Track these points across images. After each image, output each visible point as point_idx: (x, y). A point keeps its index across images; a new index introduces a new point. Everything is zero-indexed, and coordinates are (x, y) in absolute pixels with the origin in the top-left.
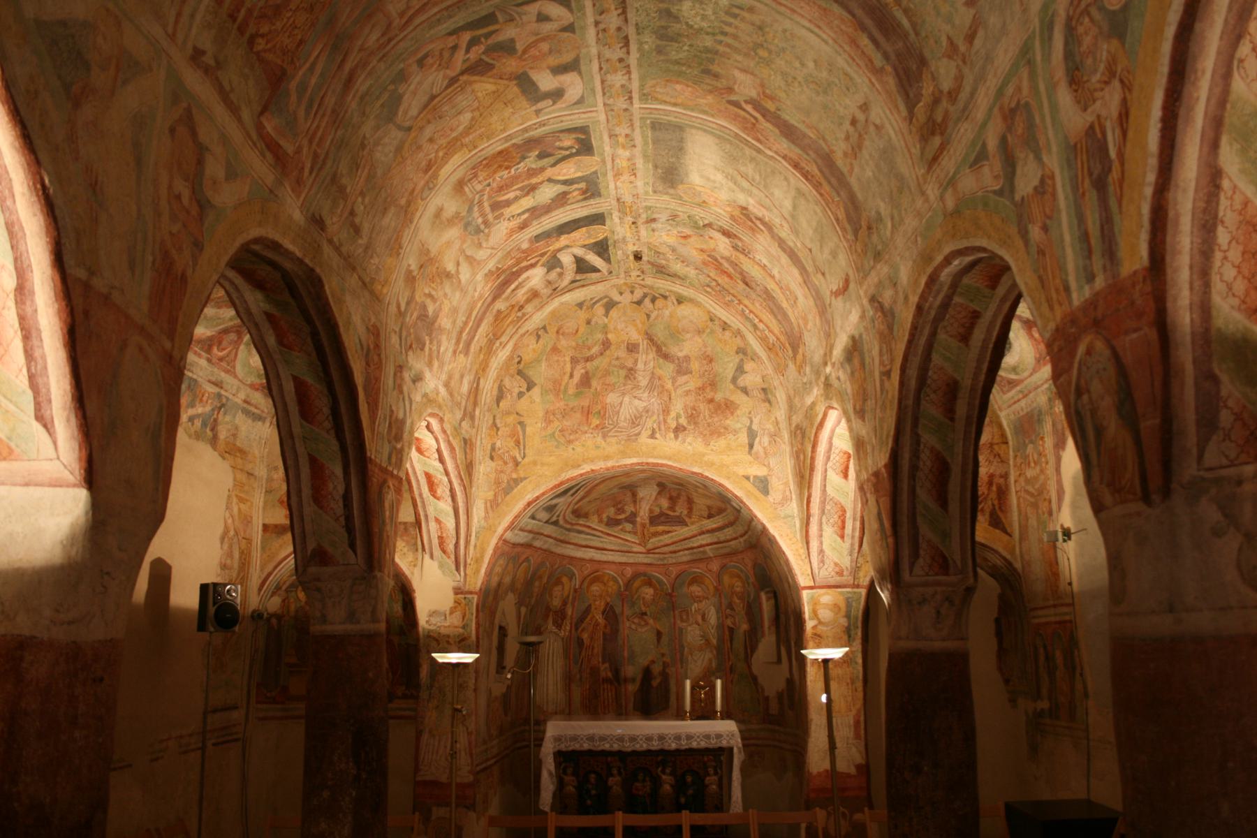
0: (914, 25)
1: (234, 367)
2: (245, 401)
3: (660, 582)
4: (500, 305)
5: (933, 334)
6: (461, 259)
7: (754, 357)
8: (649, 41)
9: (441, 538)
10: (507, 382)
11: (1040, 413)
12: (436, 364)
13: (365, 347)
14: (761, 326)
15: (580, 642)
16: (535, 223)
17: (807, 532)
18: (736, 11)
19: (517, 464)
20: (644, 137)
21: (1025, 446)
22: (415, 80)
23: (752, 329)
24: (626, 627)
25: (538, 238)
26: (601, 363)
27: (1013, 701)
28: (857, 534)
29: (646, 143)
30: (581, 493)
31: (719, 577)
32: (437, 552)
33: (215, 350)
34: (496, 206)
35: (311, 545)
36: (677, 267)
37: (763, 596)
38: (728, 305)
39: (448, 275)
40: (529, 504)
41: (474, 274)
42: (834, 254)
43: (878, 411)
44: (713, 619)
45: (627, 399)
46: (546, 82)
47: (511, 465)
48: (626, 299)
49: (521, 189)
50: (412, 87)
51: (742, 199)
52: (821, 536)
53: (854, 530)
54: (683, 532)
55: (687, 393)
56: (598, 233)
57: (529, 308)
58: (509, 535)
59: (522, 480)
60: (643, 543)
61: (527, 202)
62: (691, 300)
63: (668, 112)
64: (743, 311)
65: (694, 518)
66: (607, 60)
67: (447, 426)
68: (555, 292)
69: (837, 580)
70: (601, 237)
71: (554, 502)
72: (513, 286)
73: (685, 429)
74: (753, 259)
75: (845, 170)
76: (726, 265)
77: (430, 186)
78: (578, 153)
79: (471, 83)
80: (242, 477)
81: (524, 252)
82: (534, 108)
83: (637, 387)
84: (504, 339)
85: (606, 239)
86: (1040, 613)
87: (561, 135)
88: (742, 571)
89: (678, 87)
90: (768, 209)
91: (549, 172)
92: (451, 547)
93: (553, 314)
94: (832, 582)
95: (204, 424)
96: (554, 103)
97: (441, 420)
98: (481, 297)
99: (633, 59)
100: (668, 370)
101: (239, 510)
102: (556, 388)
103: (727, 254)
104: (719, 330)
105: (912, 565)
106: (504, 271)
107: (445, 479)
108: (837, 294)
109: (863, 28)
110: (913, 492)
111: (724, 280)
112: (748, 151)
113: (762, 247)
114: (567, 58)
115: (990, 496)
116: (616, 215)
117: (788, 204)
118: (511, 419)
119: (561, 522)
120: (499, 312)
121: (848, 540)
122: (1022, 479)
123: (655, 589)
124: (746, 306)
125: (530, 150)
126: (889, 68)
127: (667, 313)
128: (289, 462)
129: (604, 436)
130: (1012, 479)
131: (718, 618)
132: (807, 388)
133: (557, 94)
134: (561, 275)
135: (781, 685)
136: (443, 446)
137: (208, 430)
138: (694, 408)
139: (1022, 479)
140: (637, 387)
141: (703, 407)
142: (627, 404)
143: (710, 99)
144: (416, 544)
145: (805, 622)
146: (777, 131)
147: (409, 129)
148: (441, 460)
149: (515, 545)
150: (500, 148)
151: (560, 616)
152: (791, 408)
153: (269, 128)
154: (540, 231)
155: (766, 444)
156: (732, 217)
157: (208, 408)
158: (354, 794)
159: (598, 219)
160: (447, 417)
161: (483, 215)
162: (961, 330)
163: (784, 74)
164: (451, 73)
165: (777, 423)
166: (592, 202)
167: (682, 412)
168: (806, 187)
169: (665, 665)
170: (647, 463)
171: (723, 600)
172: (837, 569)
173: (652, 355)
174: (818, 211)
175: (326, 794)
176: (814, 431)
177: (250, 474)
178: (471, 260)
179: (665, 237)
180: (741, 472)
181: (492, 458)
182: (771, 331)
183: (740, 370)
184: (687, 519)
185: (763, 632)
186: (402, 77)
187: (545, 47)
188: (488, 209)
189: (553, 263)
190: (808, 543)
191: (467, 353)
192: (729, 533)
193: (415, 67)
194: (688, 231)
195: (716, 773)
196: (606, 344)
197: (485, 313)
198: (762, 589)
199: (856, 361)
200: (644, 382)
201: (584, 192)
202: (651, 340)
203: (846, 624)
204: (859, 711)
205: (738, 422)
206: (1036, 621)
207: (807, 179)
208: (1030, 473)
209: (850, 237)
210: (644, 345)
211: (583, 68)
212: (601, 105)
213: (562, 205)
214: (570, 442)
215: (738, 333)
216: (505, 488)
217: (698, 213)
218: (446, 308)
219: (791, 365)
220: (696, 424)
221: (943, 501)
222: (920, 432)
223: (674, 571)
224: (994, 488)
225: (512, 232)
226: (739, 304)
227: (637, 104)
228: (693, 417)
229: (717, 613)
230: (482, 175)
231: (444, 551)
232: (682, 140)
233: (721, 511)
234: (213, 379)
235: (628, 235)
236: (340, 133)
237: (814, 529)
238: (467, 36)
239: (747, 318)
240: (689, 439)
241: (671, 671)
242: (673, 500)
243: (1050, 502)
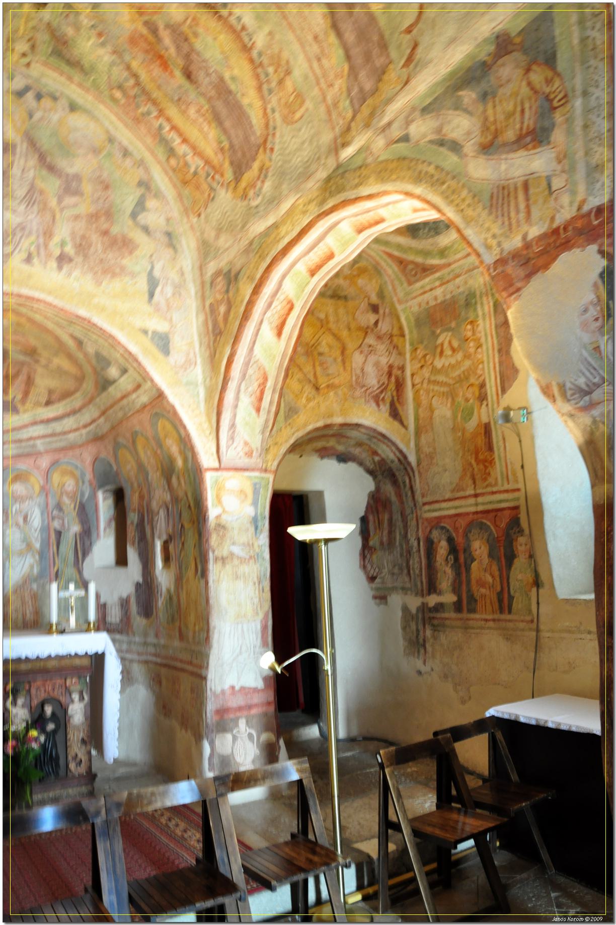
7: (158, 195)
14: (182, 149)
23: (162, 156)
27: (381, 598)
28: (274, 409)
31: (47, 475)
37: (100, 495)
44: (36, 520)
52: (236, 406)
53: (271, 403)
55: (77, 217)
62: (86, 111)
64: (161, 128)
65: (28, 405)
69: (245, 461)
73: (70, 260)
76: (167, 40)
88: (77, 467)
100: (51, 186)
104: (118, 155)
115: (389, 388)
121: (263, 413)
124: (168, 120)
127: (55, 117)
130: (408, 373)
131: (43, 521)
138: (83, 237)
141: (95, 238)
145: (206, 510)
155: (169, 295)
165: (182, 274)
167: (68, 239)
170: (19, 296)
171: (50, 501)
172: (247, 449)
173: (33, 162)
176: (264, 265)
180: (139, 323)
182: (197, 152)
183: (140, 205)
184: (19, 406)
185: (98, 535)
192: (69, 423)
195: (82, 698)
198: (101, 486)
203: (253, 514)
204: (266, 615)
205: (137, 263)
215: (141, 163)
220: (86, 256)
224: (393, 379)
226: (157, 117)
228: (83, 247)
229: (42, 514)
237: (229, 396)
239: (163, 141)
240: (76, 273)
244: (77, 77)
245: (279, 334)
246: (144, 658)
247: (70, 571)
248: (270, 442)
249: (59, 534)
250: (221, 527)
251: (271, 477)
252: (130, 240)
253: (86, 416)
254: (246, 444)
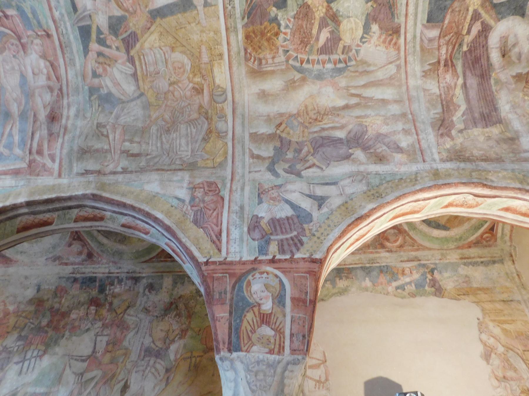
49: (323, 24)
79: (142, 47)
82: (200, 8)
150: (241, 36)
193: (96, 81)
238: (94, 46)
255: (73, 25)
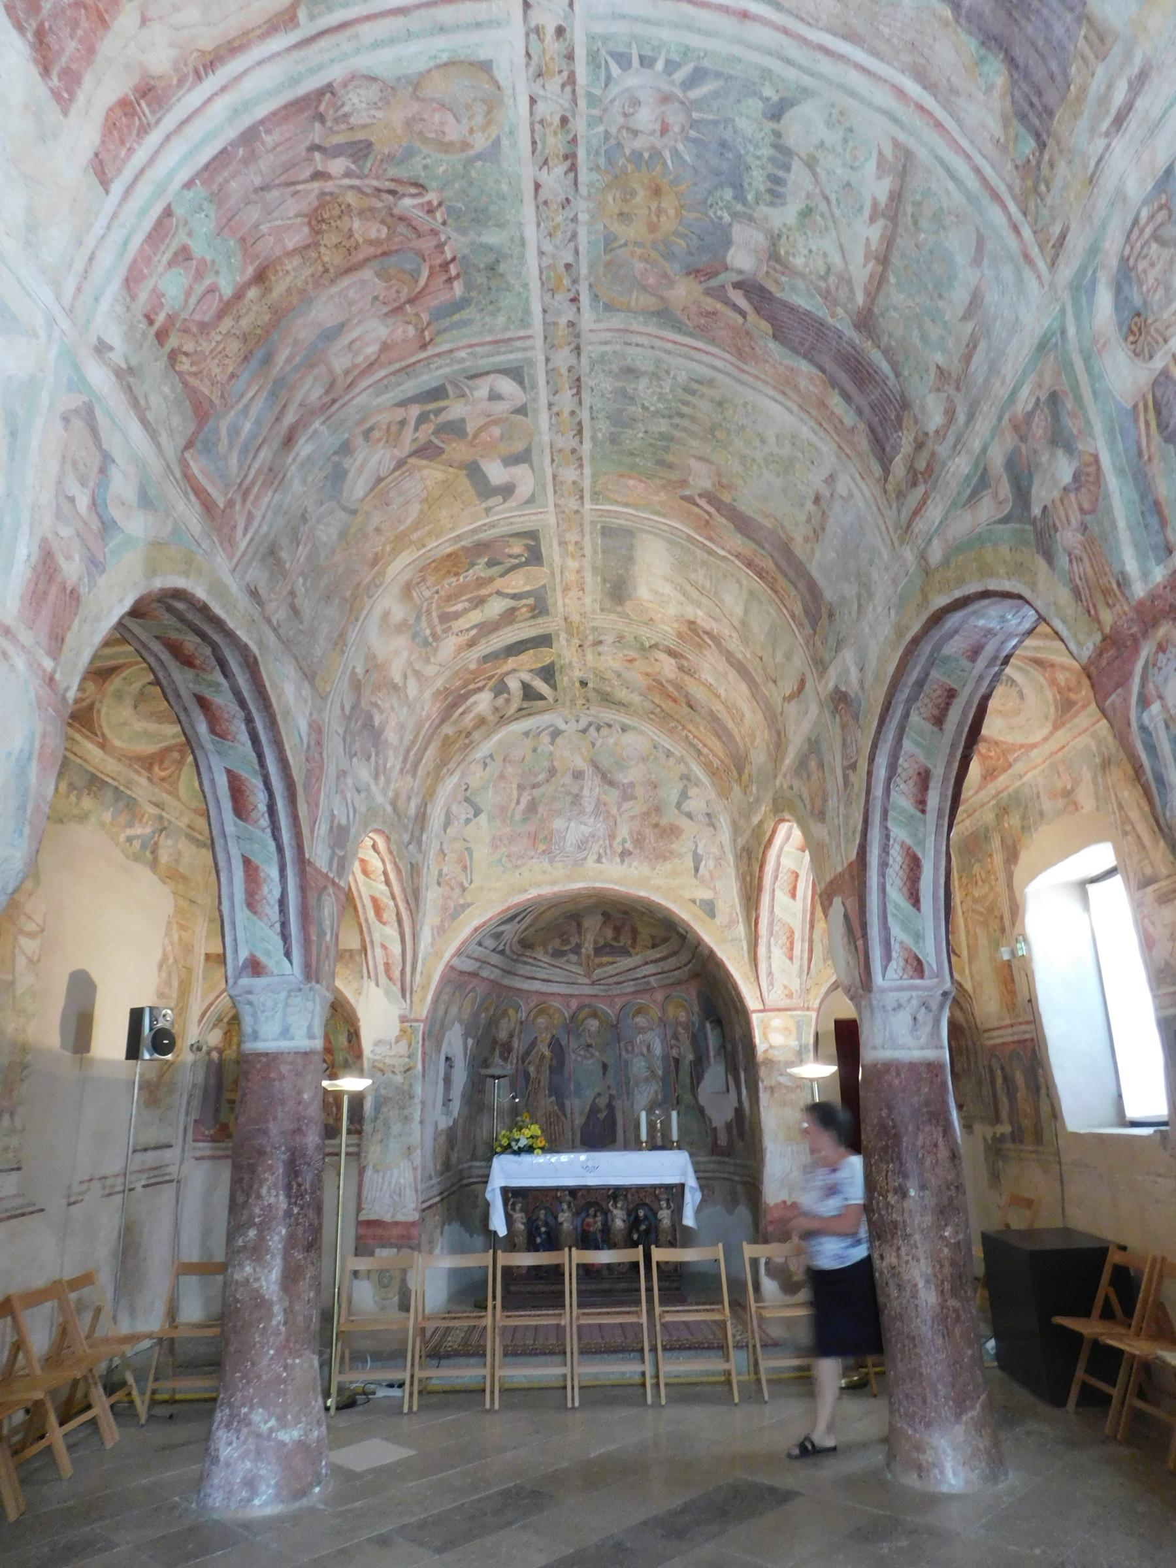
0: (894, 365)
1: (177, 789)
2: (189, 827)
3: (606, 1014)
4: (448, 729)
5: (906, 716)
6: (409, 672)
8: (603, 426)
9: (387, 965)
10: (454, 808)
11: (987, 829)
12: (382, 779)
13: (305, 740)
14: (705, 751)
15: (527, 1075)
16: (483, 641)
17: (755, 953)
18: (695, 386)
19: (464, 889)
20: (594, 544)
21: (971, 866)
22: (360, 456)
24: (573, 1059)
25: (486, 659)
26: (547, 790)
28: (806, 955)
29: (595, 553)
30: (527, 921)
31: (663, 1008)
32: (383, 979)
33: (156, 769)
34: (445, 618)
35: (243, 955)
36: (622, 694)
37: (708, 1026)
38: (671, 731)
39: (395, 687)
40: (476, 930)
41: (421, 692)
42: (788, 657)
43: (842, 807)
44: (658, 1049)
45: (573, 824)
46: (496, 473)
47: (458, 890)
48: (570, 728)
49: (469, 600)
50: (358, 463)
51: (691, 612)
54: (626, 962)
55: (633, 818)
56: (545, 656)
57: (476, 735)
58: (456, 962)
59: (469, 905)
60: (588, 974)
61: (476, 617)
62: (634, 728)
63: (621, 513)
66: (560, 451)
67: (394, 847)
68: (503, 720)
69: (787, 1003)
70: (548, 661)
71: (501, 928)
72: (461, 710)
73: (630, 853)
74: (699, 680)
75: (803, 558)
77: (375, 584)
78: (527, 563)
79: (420, 468)
80: (185, 904)
81: (472, 672)
82: (484, 505)
83: (582, 813)
84: (451, 766)
85: (552, 664)
86: (995, 1033)
87: (511, 540)
89: (631, 483)
90: (716, 620)
91: (499, 584)
92: (397, 974)
93: (500, 742)
94: (783, 1003)
95: (144, 846)
96: (505, 500)
97: (388, 839)
98: (428, 718)
99: (587, 446)
100: (613, 796)
101: (180, 938)
102: (503, 812)
103: (671, 676)
105: (885, 969)
106: (452, 692)
107: (391, 903)
108: (789, 699)
109: (833, 383)
110: (883, 890)
111: (668, 705)
112: (699, 553)
113: (710, 666)
114: (519, 446)
116: (563, 636)
117: (739, 610)
118: (458, 845)
119: (508, 952)
120: (447, 736)
122: (969, 900)
123: (601, 1022)
125: (479, 556)
126: (862, 426)
127: (611, 741)
128: (222, 864)
129: (551, 861)
132: (752, 808)
133: (507, 490)
134: (508, 701)
135: (729, 1115)
136: (389, 867)
137: (148, 853)
138: (639, 833)
139: (969, 898)
140: (582, 813)
141: (648, 832)
142: (572, 830)
143: (663, 496)
144: (361, 972)
146: (731, 526)
147: (354, 512)
148: (388, 882)
149: (462, 973)
150: (449, 550)
151: (507, 1048)
152: (736, 830)
153: (195, 468)
154: (488, 650)
156: (680, 635)
157: (148, 830)
158: (284, 1231)
159: (544, 641)
160: (394, 837)
161: (433, 628)
162: (936, 712)
163: (743, 458)
164: (399, 453)
166: (540, 620)
168: (758, 585)
169: (611, 1098)
173: (597, 781)
174: (771, 610)
175: (252, 1233)
177: (192, 901)
178: (417, 674)
179: (610, 660)
180: (687, 895)
181: (439, 884)
183: (684, 795)
186: (346, 449)
187: (496, 431)
188: (436, 621)
189: (501, 689)
190: (756, 966)
191: (414, 775)
192: (672, 962)
193: (360, 440)
194: (632, 654)
195: (668, 1207)
196: (552, 772)
197: (433, 734)
199: (813, 765)
200: (589, 808)
201: (533, 608)
202: (597, 767)
205: (683, 846)
206: (992, 1042)
207: (761, 577)
208: (977, 893)
209: (810, 631)
210: (589, 772)
211: (535, 457)
212: (551, 508)
213: (511, 623)
214: (517, 867)
216: (454, 913)
217: (645, 633)
218: (393, 723)
219: (736, 788)
221: (915, 899)
222: (889, 825)
223: (619, 1003)
225: (459, 650)
227: (588, 506)
228: (639, 841)
230: (431, 580)
231: (390, 979)
232: (631, 548)
233: (665, 940)
234: (154, 799)
235: (575, 659)
236: (278, 496)
237: (762, 951)
238: (415, 411)
239: (692, 745)
240: (635, 864)
241: (618, 1104)
242: (617, 930)
243: (1002, 918)
244: (622, 709)
245: (793, 895)
246: (746, 1179)
247: (687, 1097)
248: (810, 983)
249: (677, 1061)
250: (770, 1063)
251: (814, 1014)
252: (677, 827)
253: (684, 957)
254: (785, 987)
255: (446, 377)
